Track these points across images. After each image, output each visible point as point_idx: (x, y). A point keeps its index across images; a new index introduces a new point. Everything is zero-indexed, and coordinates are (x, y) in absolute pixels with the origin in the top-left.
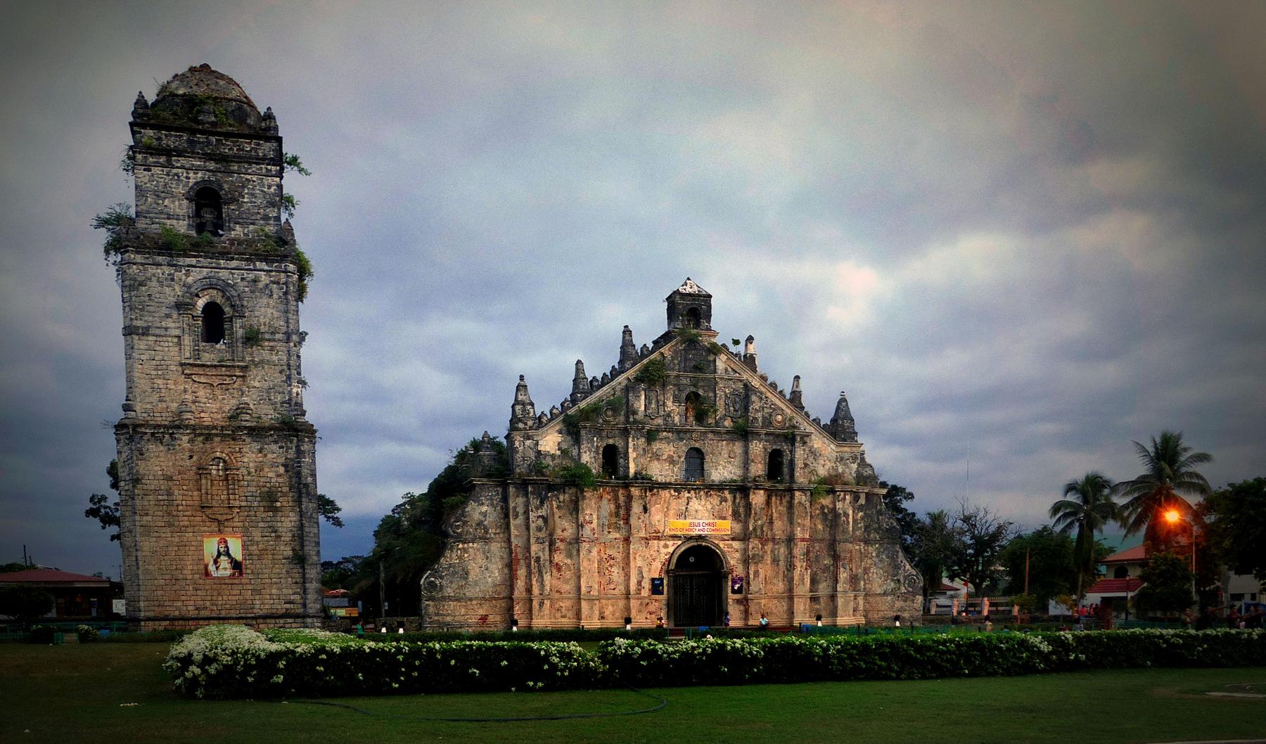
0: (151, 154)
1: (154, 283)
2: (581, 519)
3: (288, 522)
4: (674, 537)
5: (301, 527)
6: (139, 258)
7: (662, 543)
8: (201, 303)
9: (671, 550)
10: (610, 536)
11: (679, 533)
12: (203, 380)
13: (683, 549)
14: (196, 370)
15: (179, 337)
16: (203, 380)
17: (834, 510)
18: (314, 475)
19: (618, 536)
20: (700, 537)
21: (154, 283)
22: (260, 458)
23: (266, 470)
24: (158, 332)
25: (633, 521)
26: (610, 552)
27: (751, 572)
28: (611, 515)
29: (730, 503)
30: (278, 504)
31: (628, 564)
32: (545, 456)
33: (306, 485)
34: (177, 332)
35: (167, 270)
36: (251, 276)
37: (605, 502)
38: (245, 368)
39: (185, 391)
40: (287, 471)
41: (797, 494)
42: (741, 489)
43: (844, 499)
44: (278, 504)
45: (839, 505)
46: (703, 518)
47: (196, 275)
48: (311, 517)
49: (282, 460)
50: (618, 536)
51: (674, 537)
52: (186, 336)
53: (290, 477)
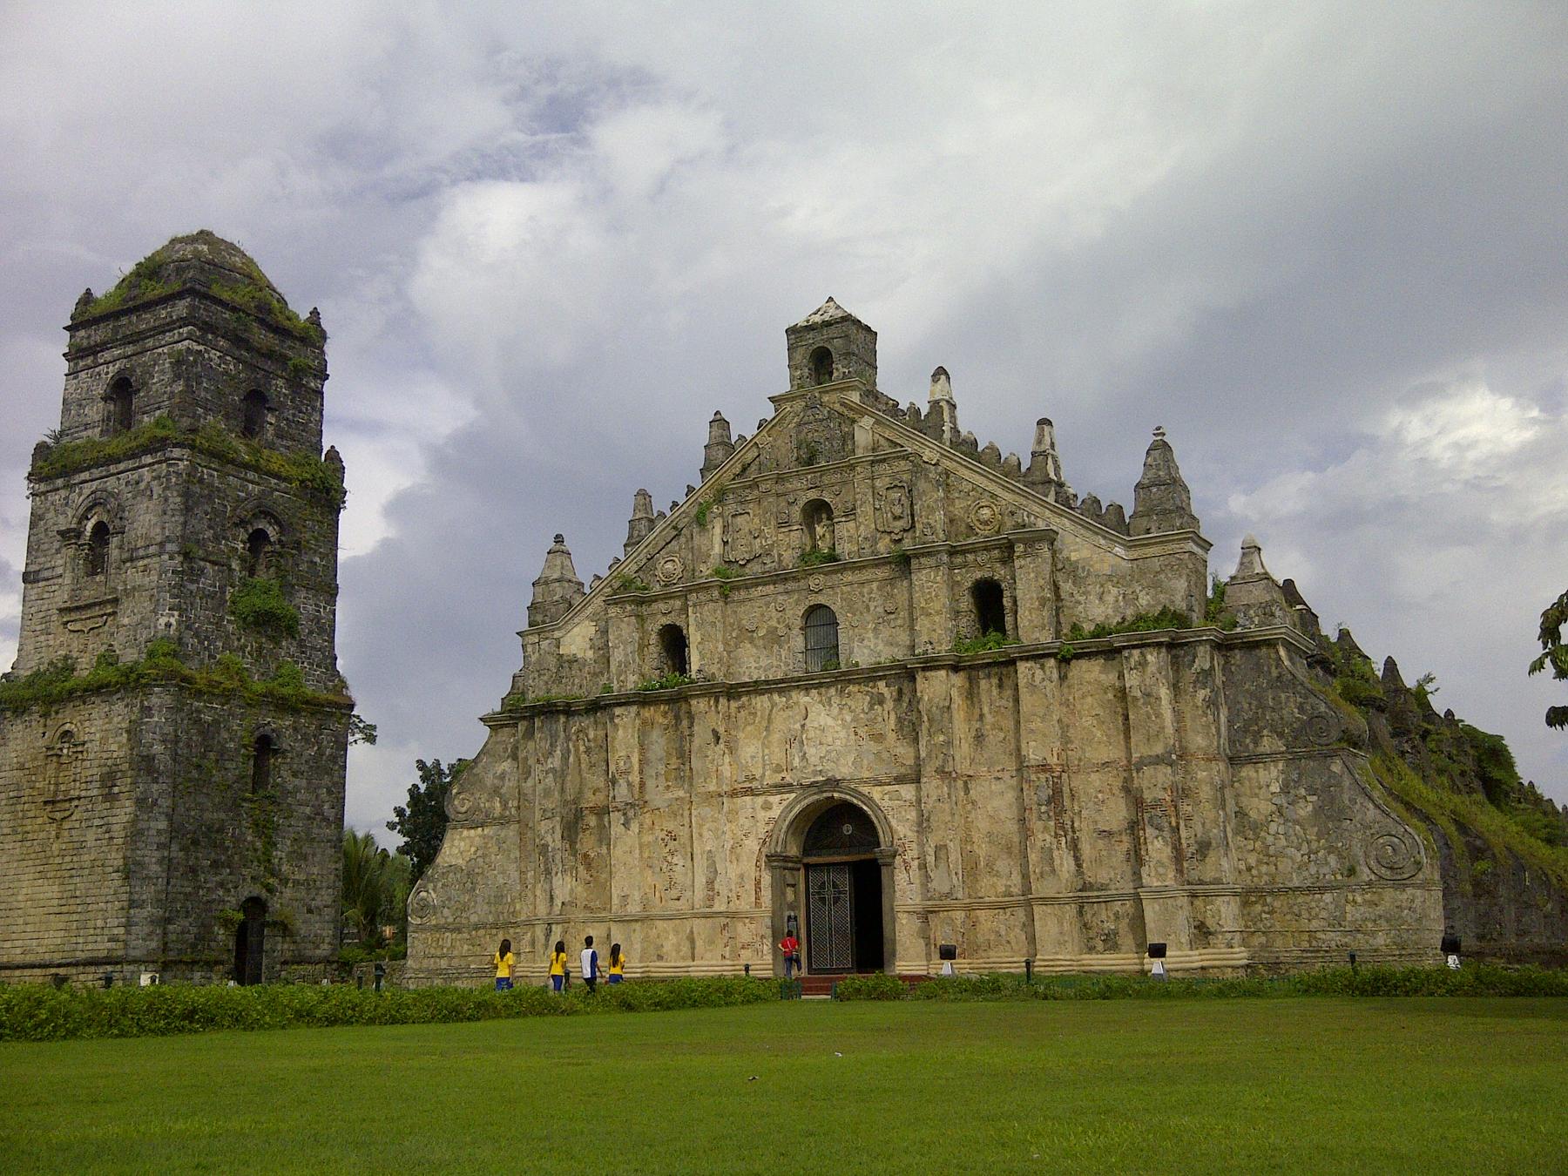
0: (82, 358)
1: (51, 514)
2: (612, 768)
3: (124, 812)
5: (134, 822)
6: (43, 487)
7: (760, 800)
8: (90, 525)
9: (776, 812)
11: (788, 779)
12: (78, 626)
13: (797, 810)
14: (74, 616)
16: (78, 626)
17: (1122, 694)
20: (833, 783)
21: (51, 514)
24: (46, 574)
26: (670, 826)
28: (669, 754)
29: (889, 705)
32: (570, 662)
33: (150, 759)
34: (60, 571)
35: (63, 493)
36: (134, 476)
37: (655, 735)
38: (116, 601)
39: (61, 645)
42: (905, 674)
43: (1143, 664)
44: (116, 790)
45: (1132, 680)
46: (832, 739)
47: (88, 489)
48: (155, 803)
50: (681, 793)
53: (132, 749)
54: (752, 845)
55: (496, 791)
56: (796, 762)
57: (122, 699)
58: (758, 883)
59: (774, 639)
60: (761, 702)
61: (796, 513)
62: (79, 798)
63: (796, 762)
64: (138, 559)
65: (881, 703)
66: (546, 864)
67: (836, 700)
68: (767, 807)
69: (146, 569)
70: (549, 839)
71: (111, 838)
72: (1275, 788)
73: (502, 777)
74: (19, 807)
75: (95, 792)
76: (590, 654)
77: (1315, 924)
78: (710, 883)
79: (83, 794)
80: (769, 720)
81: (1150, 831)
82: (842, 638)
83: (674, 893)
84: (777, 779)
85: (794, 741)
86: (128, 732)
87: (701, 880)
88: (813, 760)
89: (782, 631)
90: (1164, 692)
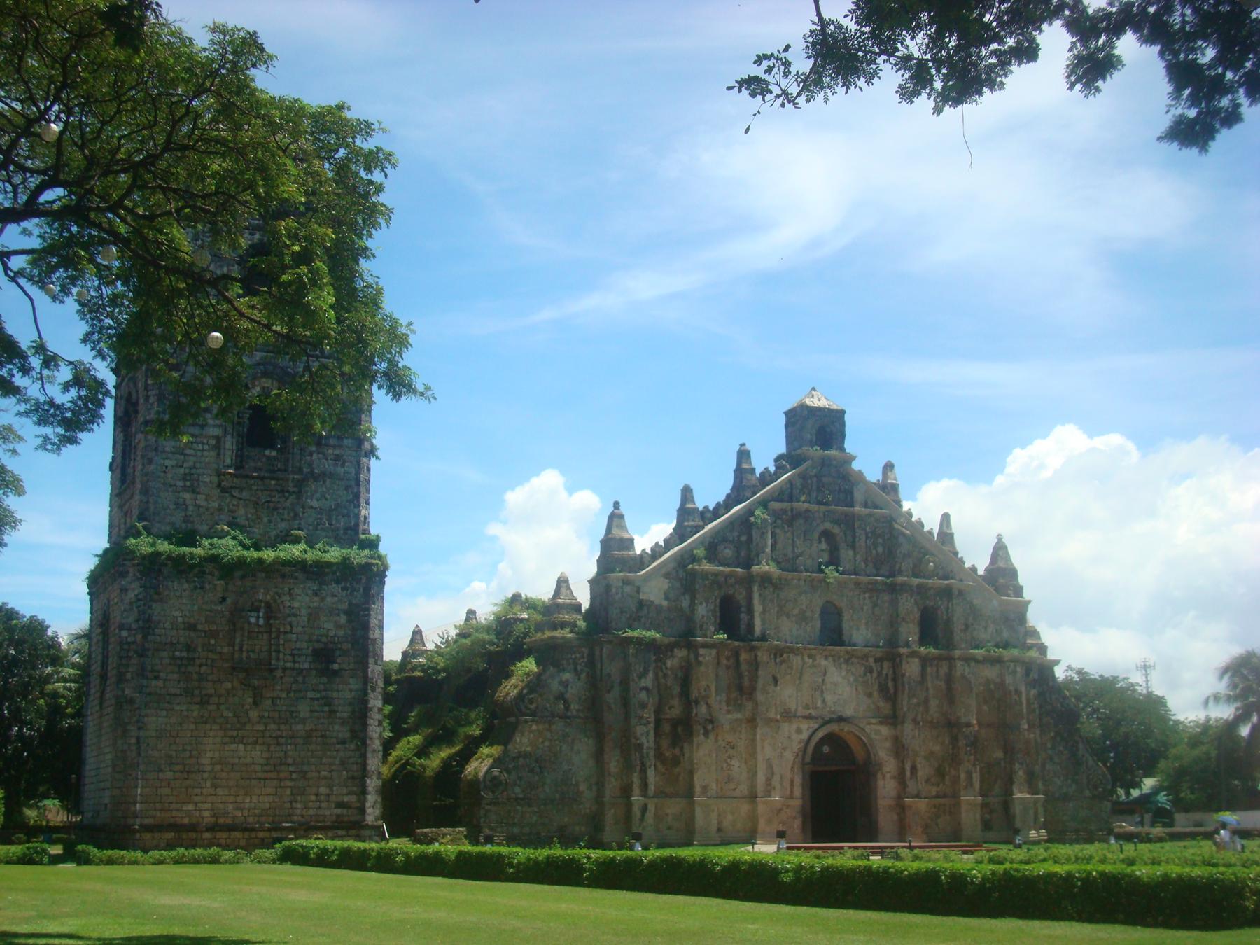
4: (809, 717)
7: (794, 727)
9: (805, 736)
10: (730, 716)
11: (813, 713)
13: (820, 734)
15: (218, 438)
18: (381, 627)
19: (739, 716)
20: (841, 719)
22: (316, 602)
23: (323, 618)
25: (760, 697)
27: (908, 767)
29: (875, 675)
30: (336, 667)
31: (753, 754)
34: (218, 432)
40: (349, 621)
41: (959, 664)
43: (1015, 672)
44: (336, 667)
45: (1009, 680)
49: (344, 606)
50: (739, 716)
51: (809, 717)
52: (229, 437)
54: (789, 756)
55: (561, 697)
56: (819, 704)
57: (338, 582)
58: (792, 782)
59: (803, 618)
60: (796, 660)
61: (816, 536)
62: (284, 669)
63: (819, 704)
64: (327, 445)
65: (871, 672)
66: (642, 757)
67: (844, 666)
68: (799, 731)
69: (337, 458)
70: (644, 740)
71: (332, 712)
72: (1049, 746)
73: (566, 684)
74: (190, 669)
75: (306, 666)
76: (665, 603)
77: (1065, 818)
78: (769, 781)
79: (289, 665)
80: (801, 674)
81: (1017, 766)
82: (845, 626)
83: (732, 786)
84: (807, 712)
85: (819, 689)
86: (348, 613)
87: (761, 778)
88: (829, 704)
89: (809, 614)
90: (1023, 689)
